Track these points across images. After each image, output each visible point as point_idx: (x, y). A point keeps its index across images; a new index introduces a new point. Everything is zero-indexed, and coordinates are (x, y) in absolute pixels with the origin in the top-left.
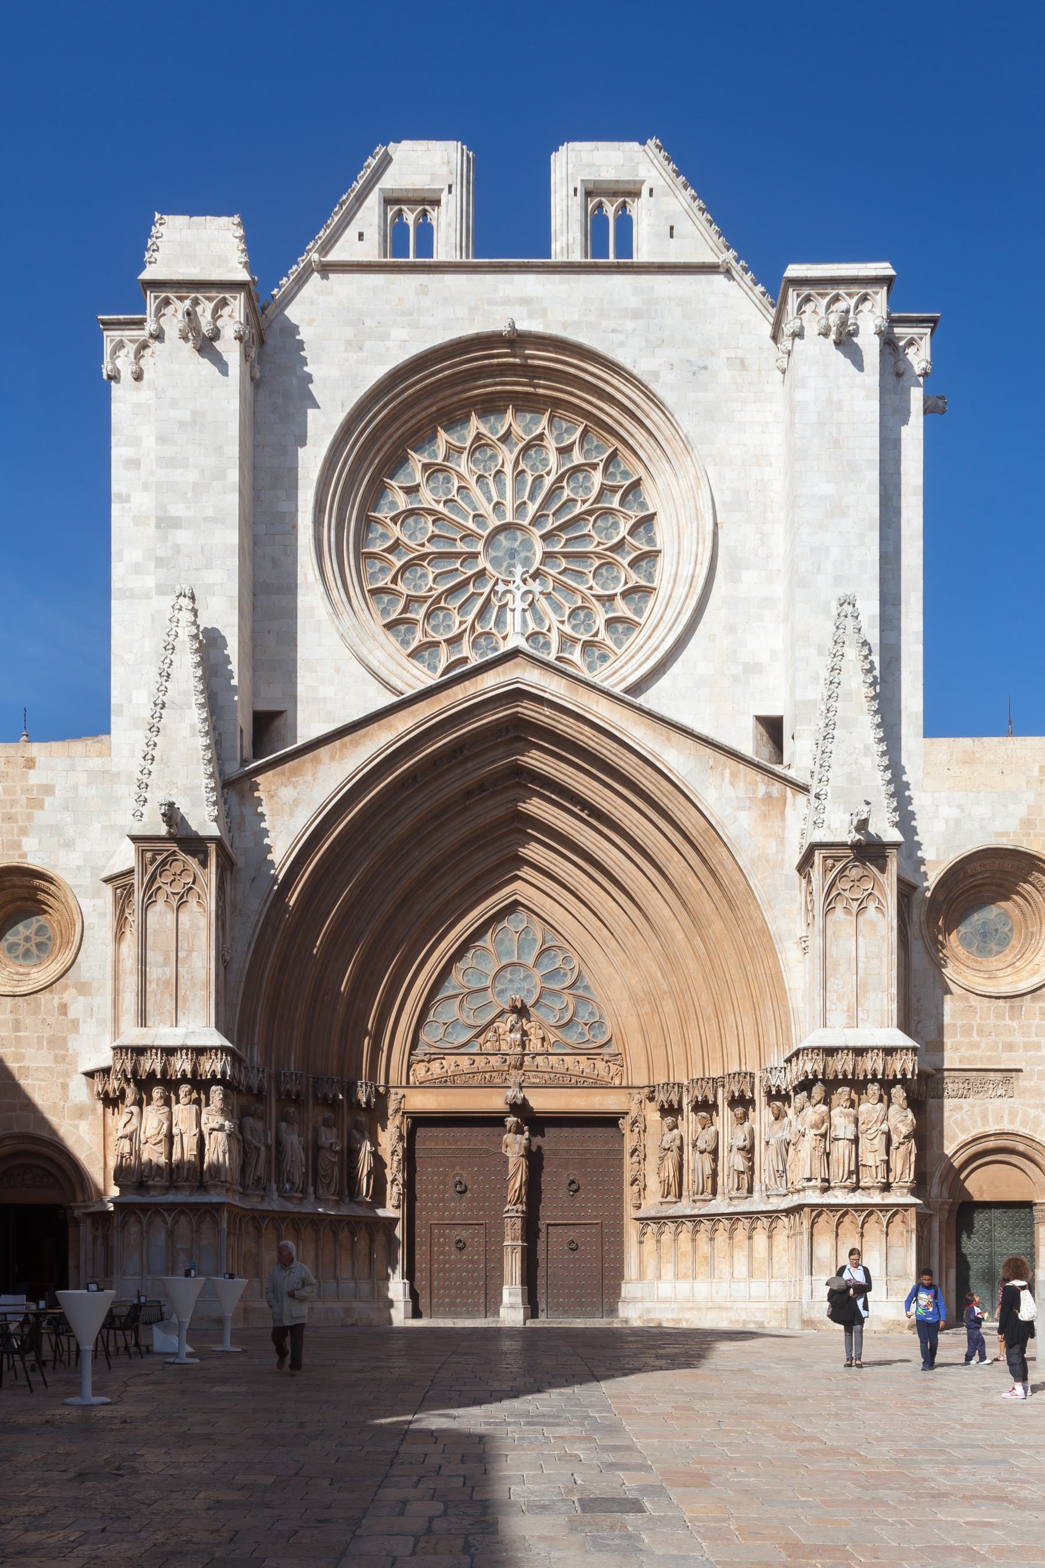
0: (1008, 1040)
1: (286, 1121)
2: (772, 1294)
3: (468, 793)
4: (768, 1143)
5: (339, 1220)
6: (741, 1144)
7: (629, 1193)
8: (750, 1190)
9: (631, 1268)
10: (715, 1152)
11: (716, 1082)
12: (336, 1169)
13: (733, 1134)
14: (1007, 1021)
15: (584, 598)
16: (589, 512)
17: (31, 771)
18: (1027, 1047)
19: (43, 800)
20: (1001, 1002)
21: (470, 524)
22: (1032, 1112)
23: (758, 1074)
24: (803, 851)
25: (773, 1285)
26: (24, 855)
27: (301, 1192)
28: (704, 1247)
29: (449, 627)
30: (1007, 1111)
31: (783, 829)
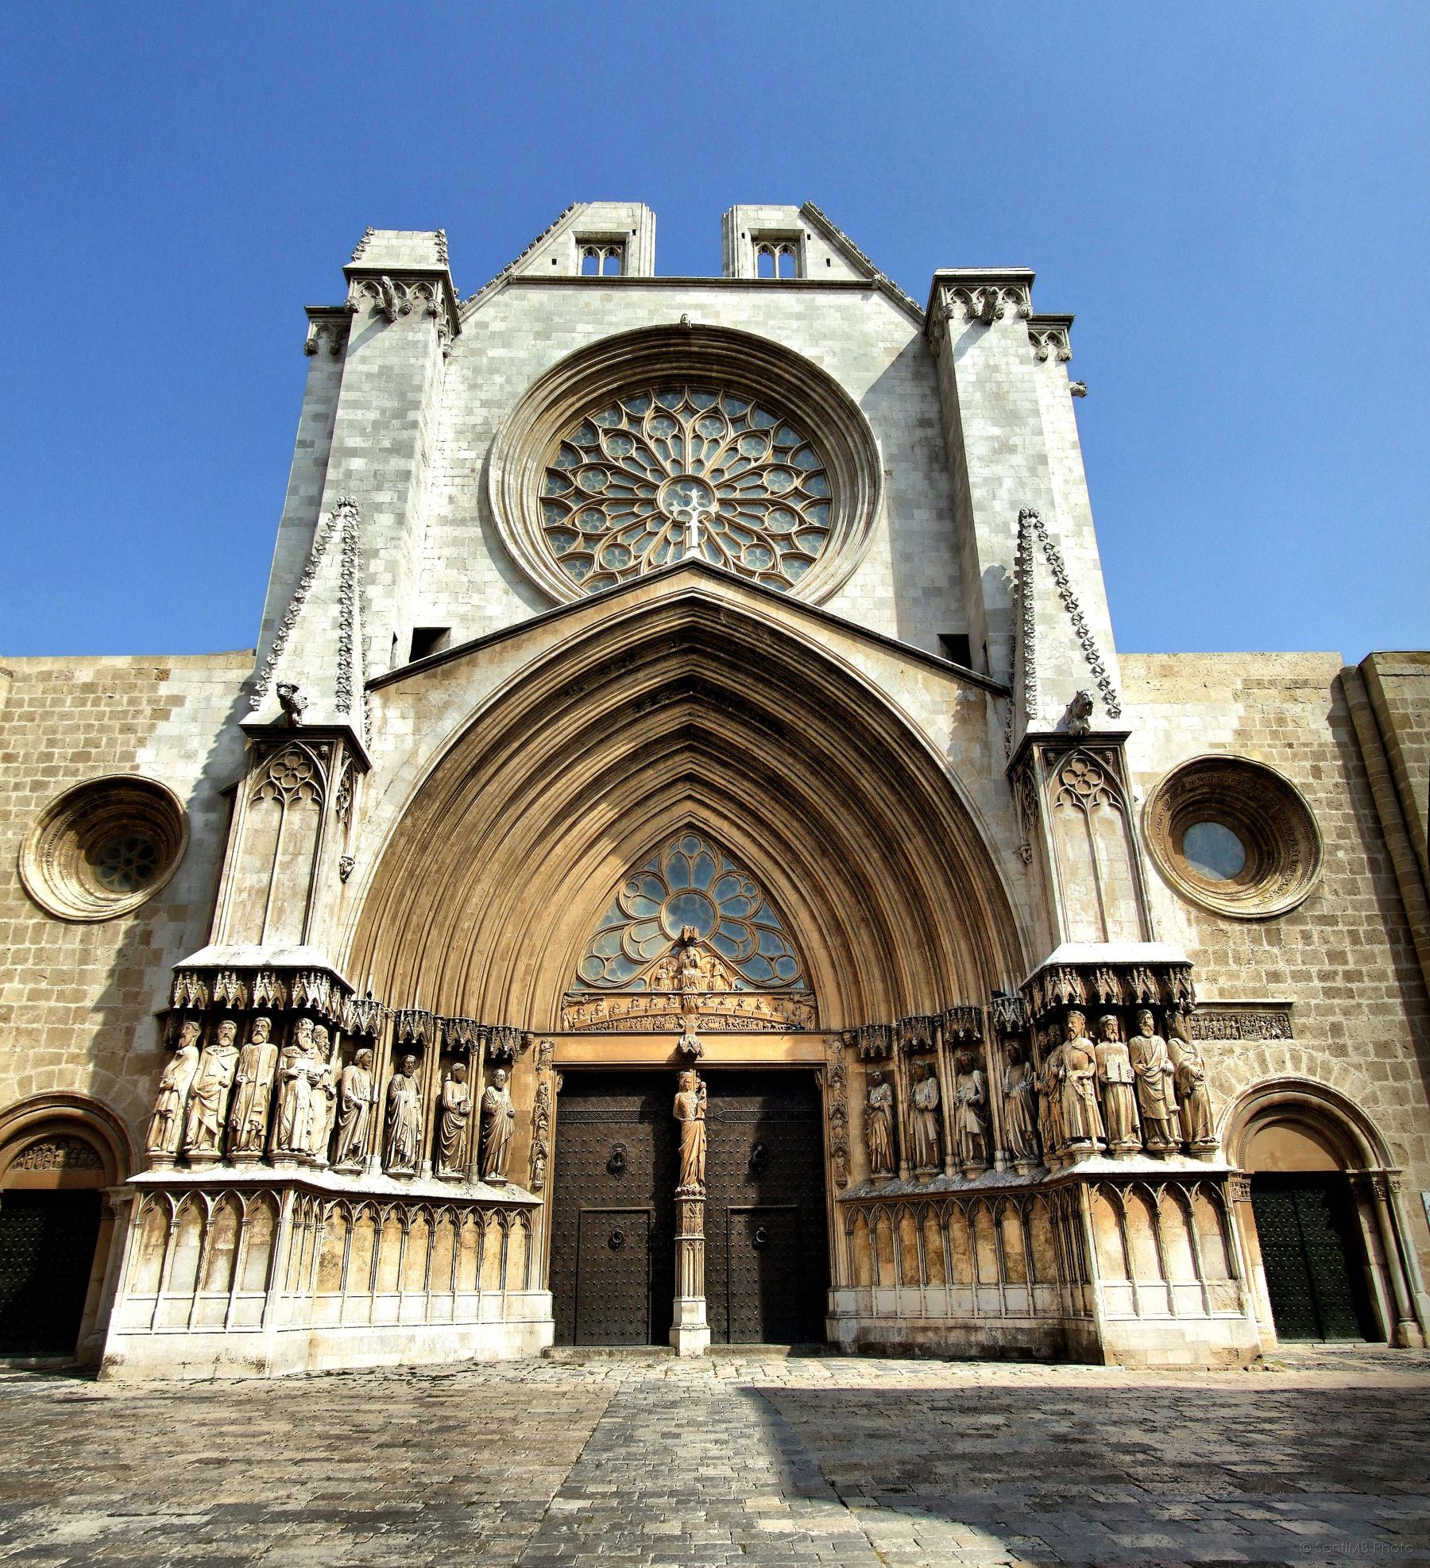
0: (1271, 968)
1: (403, 1073)
2: (1039, 1307)
3: (637, 704)
4: (1006, 1096)
5: (462, 1204)
6: (971, 1096)
7: (833, 1166)
8: (991, 1161)
9: (841, 1271)
10: (938, 1109)
11: (934, 1023)
12: (463, 1136)
13: (958, 1085)
14: (1268, 948)
15: (760, 538)
16: (763, 468)
17: (163, 684)
18: (1297, 976)
19: (169, 711)
20: (1255, 927)
21: (649, 476)
22: (1319, 1056)
23: (985, 1009)
24: (1012, 754)
25: (1038, 1293)
26: (137, 767)
27: (415, 1167)
28: (935, 1240)
29: (625, 563)
30: (1288, 1056)
31: (987, 733)
